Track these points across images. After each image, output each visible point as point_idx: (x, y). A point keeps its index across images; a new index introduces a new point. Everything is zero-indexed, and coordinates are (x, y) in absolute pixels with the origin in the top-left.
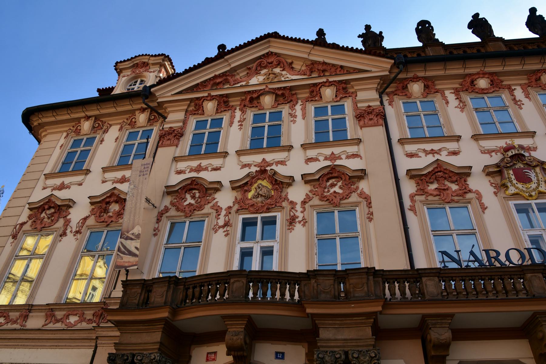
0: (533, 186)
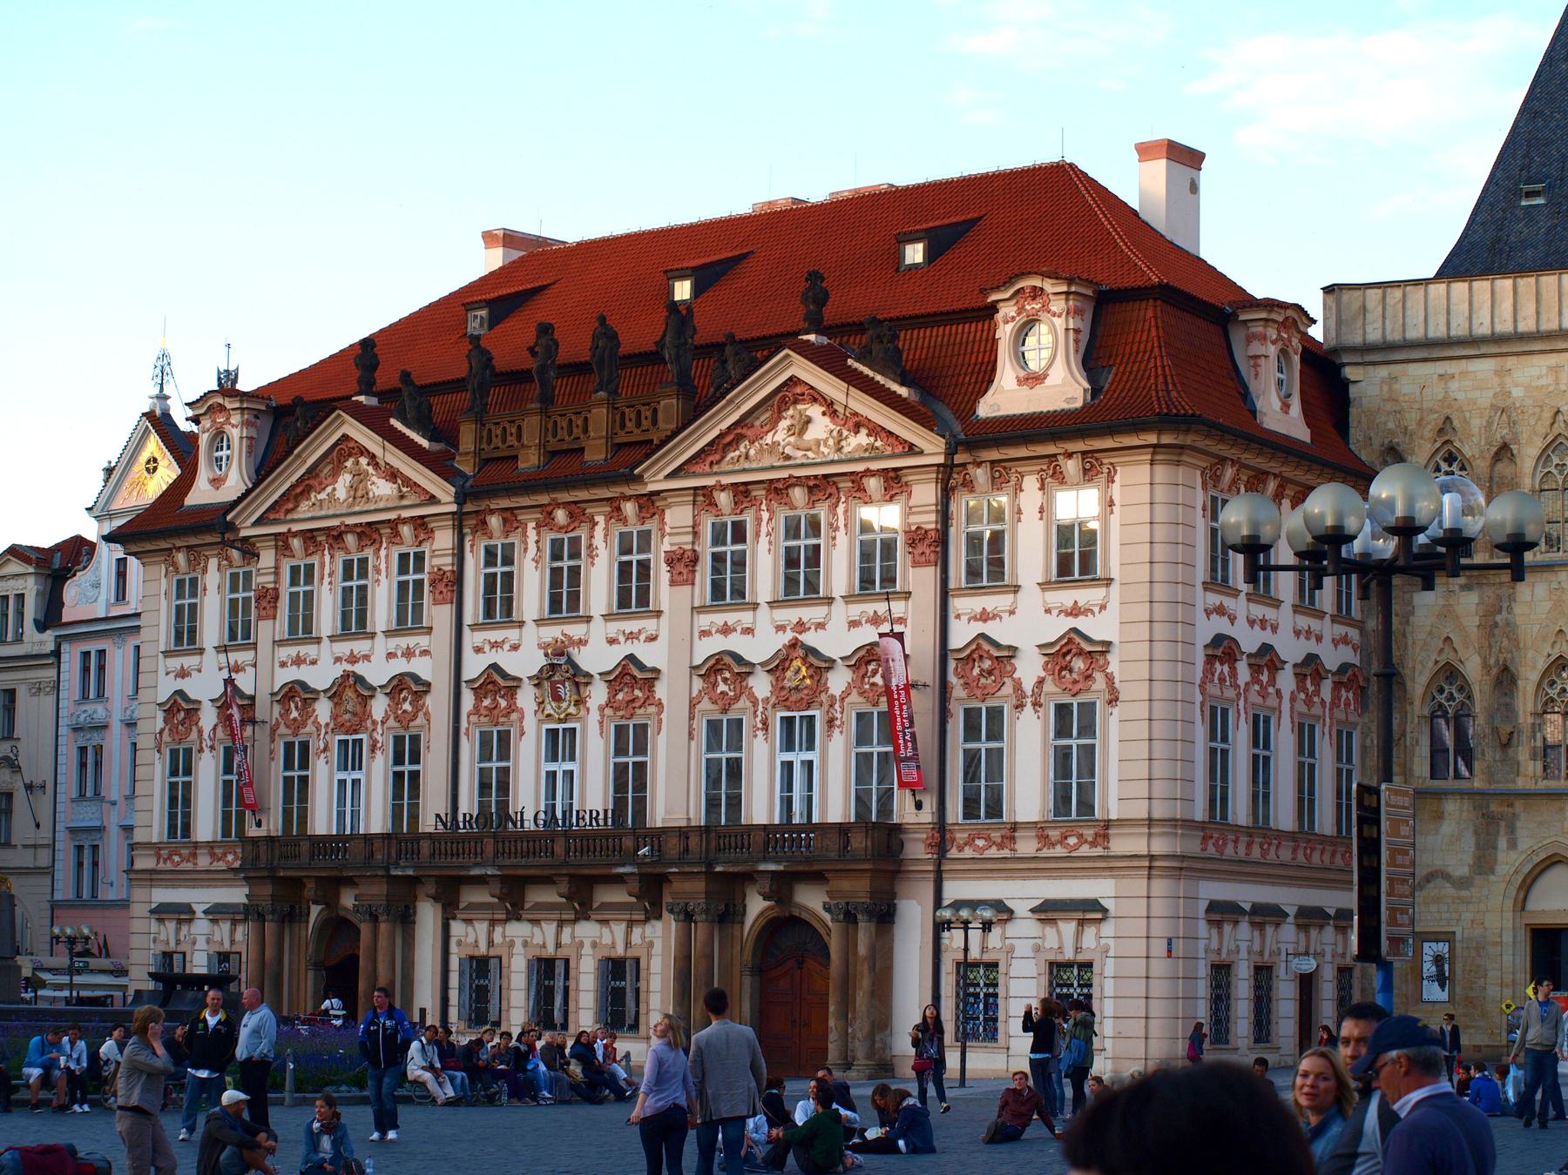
0: (564, 705)
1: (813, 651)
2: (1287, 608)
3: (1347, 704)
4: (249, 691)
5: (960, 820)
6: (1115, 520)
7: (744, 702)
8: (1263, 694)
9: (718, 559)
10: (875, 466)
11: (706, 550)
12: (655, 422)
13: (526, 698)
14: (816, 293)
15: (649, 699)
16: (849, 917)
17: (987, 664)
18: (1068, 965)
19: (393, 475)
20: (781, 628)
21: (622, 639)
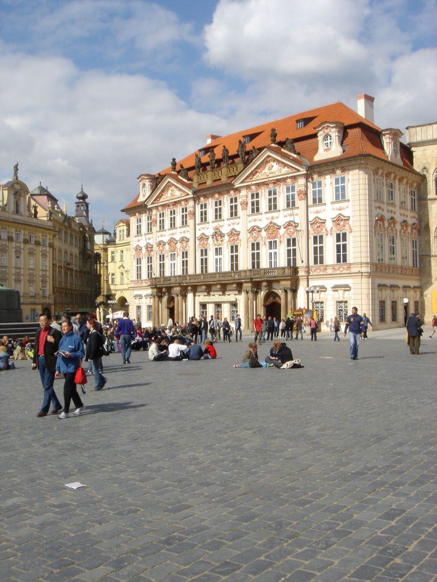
1: (275, 224)
2: (398, 207)
3: (415, 233)
4: (152, 244)
5: (313, 265)
6: (350, 184)
7: (260, 238)
8: (392, 230)
9: (253, 204)
10: (289, 176)
11: (250, 201)
12: (237, 170)
13: (210, 240)
14: (274, 135)
16: (286, 291)
17: (318, 224)
18: (341, 302)
19: (180, 189)
20: (268, 219)
21: (231, 224)
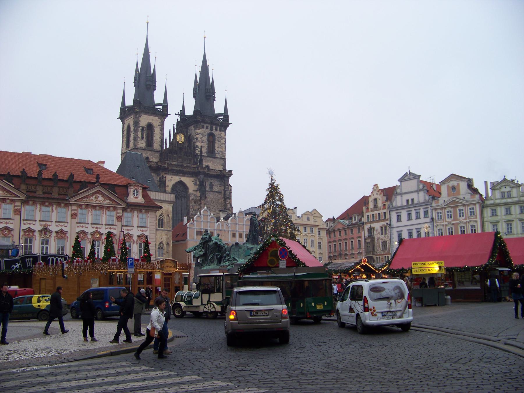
6: (149, 219)
7: (86, 238)
13: (37, 234)
15: (65, 236)
